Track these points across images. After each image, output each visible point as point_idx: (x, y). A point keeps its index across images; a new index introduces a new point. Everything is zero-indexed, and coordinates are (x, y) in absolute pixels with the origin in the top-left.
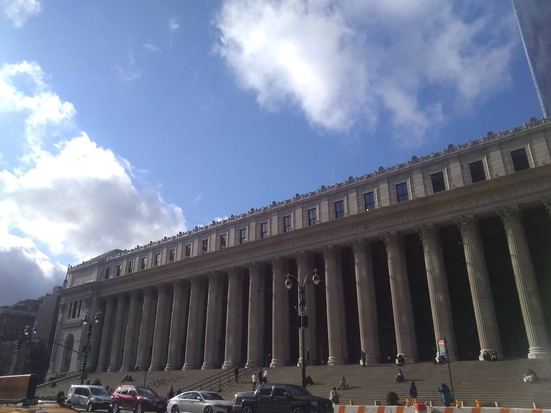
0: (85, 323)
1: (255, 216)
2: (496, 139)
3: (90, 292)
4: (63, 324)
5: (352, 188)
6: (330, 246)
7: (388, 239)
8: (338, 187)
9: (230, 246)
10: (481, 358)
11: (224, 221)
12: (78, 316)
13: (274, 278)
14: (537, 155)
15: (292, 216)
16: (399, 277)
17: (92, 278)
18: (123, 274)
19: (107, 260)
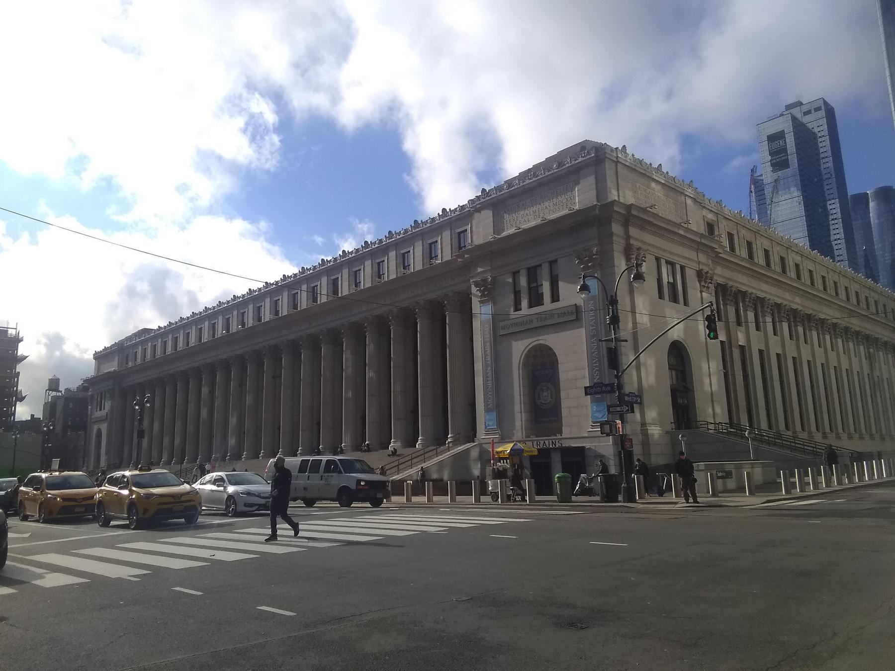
0: (148, 405)
2: (393, 239)
4: (92, 417)
8: (460, 211)
9: (391, 277)
10: (172, 464)
11: (380, 240)
12: (104, 409)
13: (447, 322)
15: (386, 261)
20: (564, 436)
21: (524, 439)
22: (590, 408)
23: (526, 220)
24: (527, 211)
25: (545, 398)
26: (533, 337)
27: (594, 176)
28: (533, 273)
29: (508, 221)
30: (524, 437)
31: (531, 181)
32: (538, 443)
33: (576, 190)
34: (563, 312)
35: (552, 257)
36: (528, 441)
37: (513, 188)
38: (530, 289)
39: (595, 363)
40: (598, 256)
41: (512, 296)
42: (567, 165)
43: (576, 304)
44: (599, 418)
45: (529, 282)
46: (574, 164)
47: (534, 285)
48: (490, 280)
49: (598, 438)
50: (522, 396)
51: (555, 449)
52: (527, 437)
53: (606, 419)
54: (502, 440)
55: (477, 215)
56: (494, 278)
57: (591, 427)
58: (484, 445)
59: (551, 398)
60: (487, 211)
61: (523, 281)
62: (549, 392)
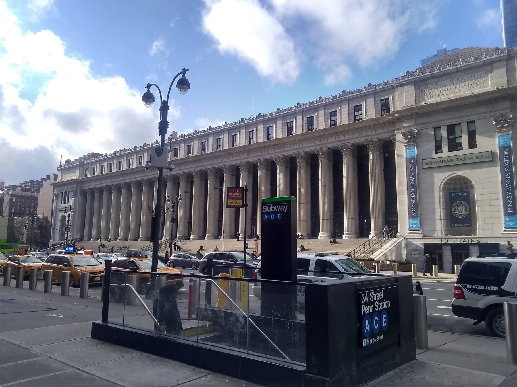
1: (183, 140)
2: (323, 102)
3: (75, 186)
5: (243, 126)
6: (282, 156)
7: (344, 150)
12: (68, 203)
14: (342, 116)
16: (263, 188)
17: (75, 175)
18: (97, 174)
19: (85, 162)
21: (444, 237)
23: (444, 93)
24: (444, 88)
26: (452, 171)
27: (506, 68)
28: (451, 129)
29: (428, 94)
31: (451, 68)
33: (489, 76)
34: (481, 156)
35: (471, 119)
37: (435, 72)
38: (449, 139)
40: (512, 120)
41: (433, 144)
42: (483, 60)
43: (492, 151)
44: (510, 225)
45: (449, 134)
46: (489, 59)
47: (453, 136)
48: (416, 132)
49: (511, 238)
52: (446, 235)
54: (424, 237)
55: (400, 88)
56: (418, 130)
57: (504, 231)
58: (408, 240)
60: (409, 86)
61: (444, 134)
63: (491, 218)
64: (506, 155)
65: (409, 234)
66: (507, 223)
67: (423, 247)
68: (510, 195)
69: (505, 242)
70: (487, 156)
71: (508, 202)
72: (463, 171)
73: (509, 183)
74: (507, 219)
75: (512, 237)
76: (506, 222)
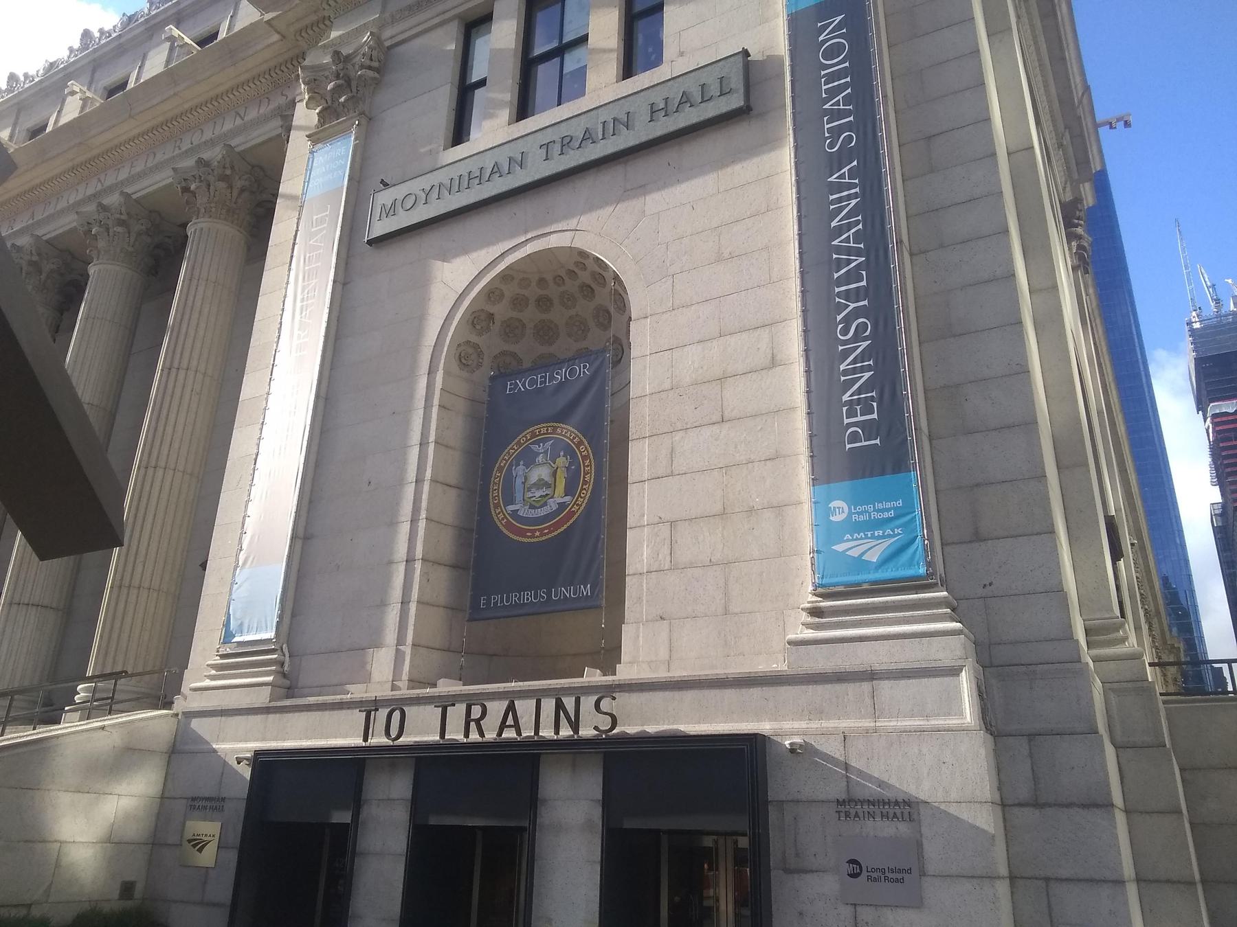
20: (625, 672)
21: (404, 692)
22: (805, 516)
25: (538, 494)
30: (403, 683)
32: (476, 712)
36: (418, 701)
39: (848, 278)
43: (746, 53)
44: (860, 563)
49: (866, 686)
50: (426, 487)
51: (575, 746)
52: (414, 682)
53: (922, 570)
59: (569, 491)
62: (562, 461)
63: (723, 514)
64: (832, 52)
65: (213, 678)
66: (839, 548)
67: (246, 772)
68: (857, 313)
69: (815, 725)
70: (714, 90)
71: (845, 373)
72: (586, 221)
73: (849, 227)
74: (840, 510)
75: (871, 676)
76: (828, 532)
